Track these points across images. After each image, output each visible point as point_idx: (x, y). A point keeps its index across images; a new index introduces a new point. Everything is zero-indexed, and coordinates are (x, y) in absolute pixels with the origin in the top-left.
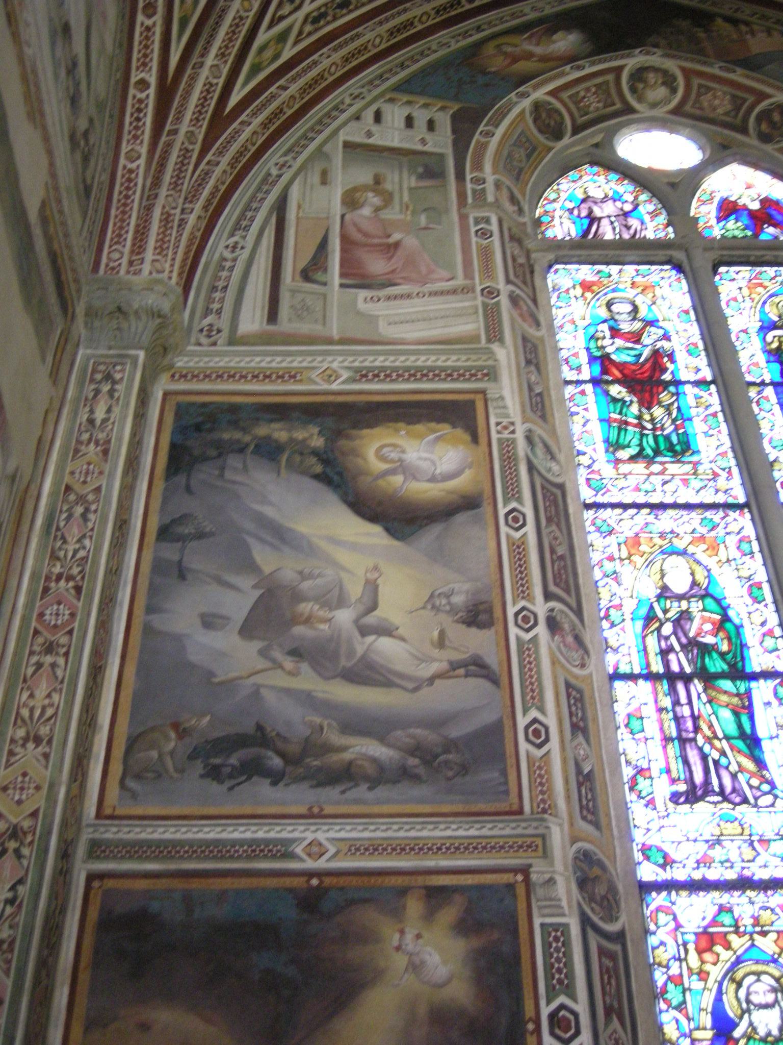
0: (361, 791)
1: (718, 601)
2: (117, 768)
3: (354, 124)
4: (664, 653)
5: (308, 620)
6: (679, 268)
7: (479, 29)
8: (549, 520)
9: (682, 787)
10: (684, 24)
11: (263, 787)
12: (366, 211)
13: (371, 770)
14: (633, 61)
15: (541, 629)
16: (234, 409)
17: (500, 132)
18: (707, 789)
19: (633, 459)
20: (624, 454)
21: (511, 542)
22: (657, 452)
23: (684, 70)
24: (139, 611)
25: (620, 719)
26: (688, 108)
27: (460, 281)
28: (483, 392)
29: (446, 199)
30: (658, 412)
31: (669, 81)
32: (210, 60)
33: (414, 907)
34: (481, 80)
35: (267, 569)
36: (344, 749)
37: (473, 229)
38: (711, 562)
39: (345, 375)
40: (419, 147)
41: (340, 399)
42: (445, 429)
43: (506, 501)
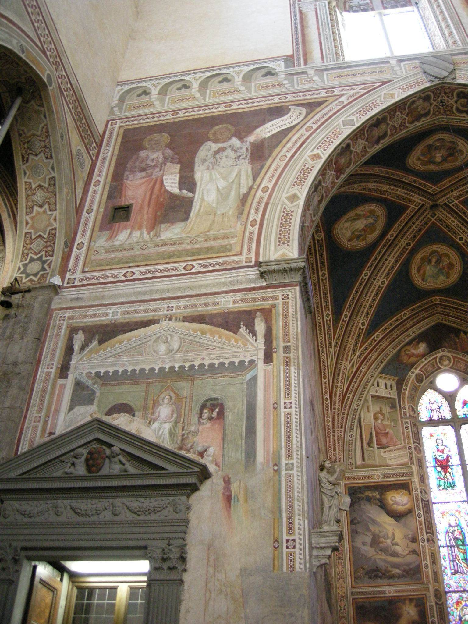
0: (396, 580)
1: (460, 527)
2: (353, 577)
3: (372, 388)
4: (450, 540)
5: (382, 543)
6: (452, 427)
7: (399, 344)
8: (426, 512)
9: (453, 571)
10: (452, 336)
11: (379, 580)
12: (379, 421)
13: (397, 575)
14: (439, 355)
15: (426, 543)
16: (360, 488)
17: (408, 388)
18: (458, 571)
19: (443, 489)
20: (441, 488)
21: (419, 521)
22: (448, 487)
23: (452, 356)
24: (350, 542)
25: (441, 556)
26: (454, 367)
27: (403, 445)
28: (410, 480)
29: (397, 415)
30: (448, 474)
31: (449, 359)
32: (339, 384)
33: (407, 602)
34: (402, 366)
35: (373, 531)
36: (392, 571)
37: (405, 426)
38: (459, 517)
39: (381, 476)
40: (389, 396)
41: (381, 484)
42: (404, 491)
43: (418, 510)
